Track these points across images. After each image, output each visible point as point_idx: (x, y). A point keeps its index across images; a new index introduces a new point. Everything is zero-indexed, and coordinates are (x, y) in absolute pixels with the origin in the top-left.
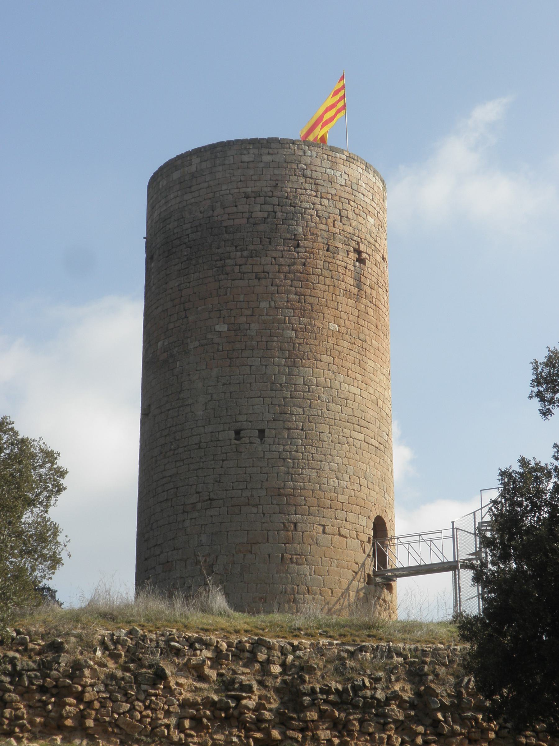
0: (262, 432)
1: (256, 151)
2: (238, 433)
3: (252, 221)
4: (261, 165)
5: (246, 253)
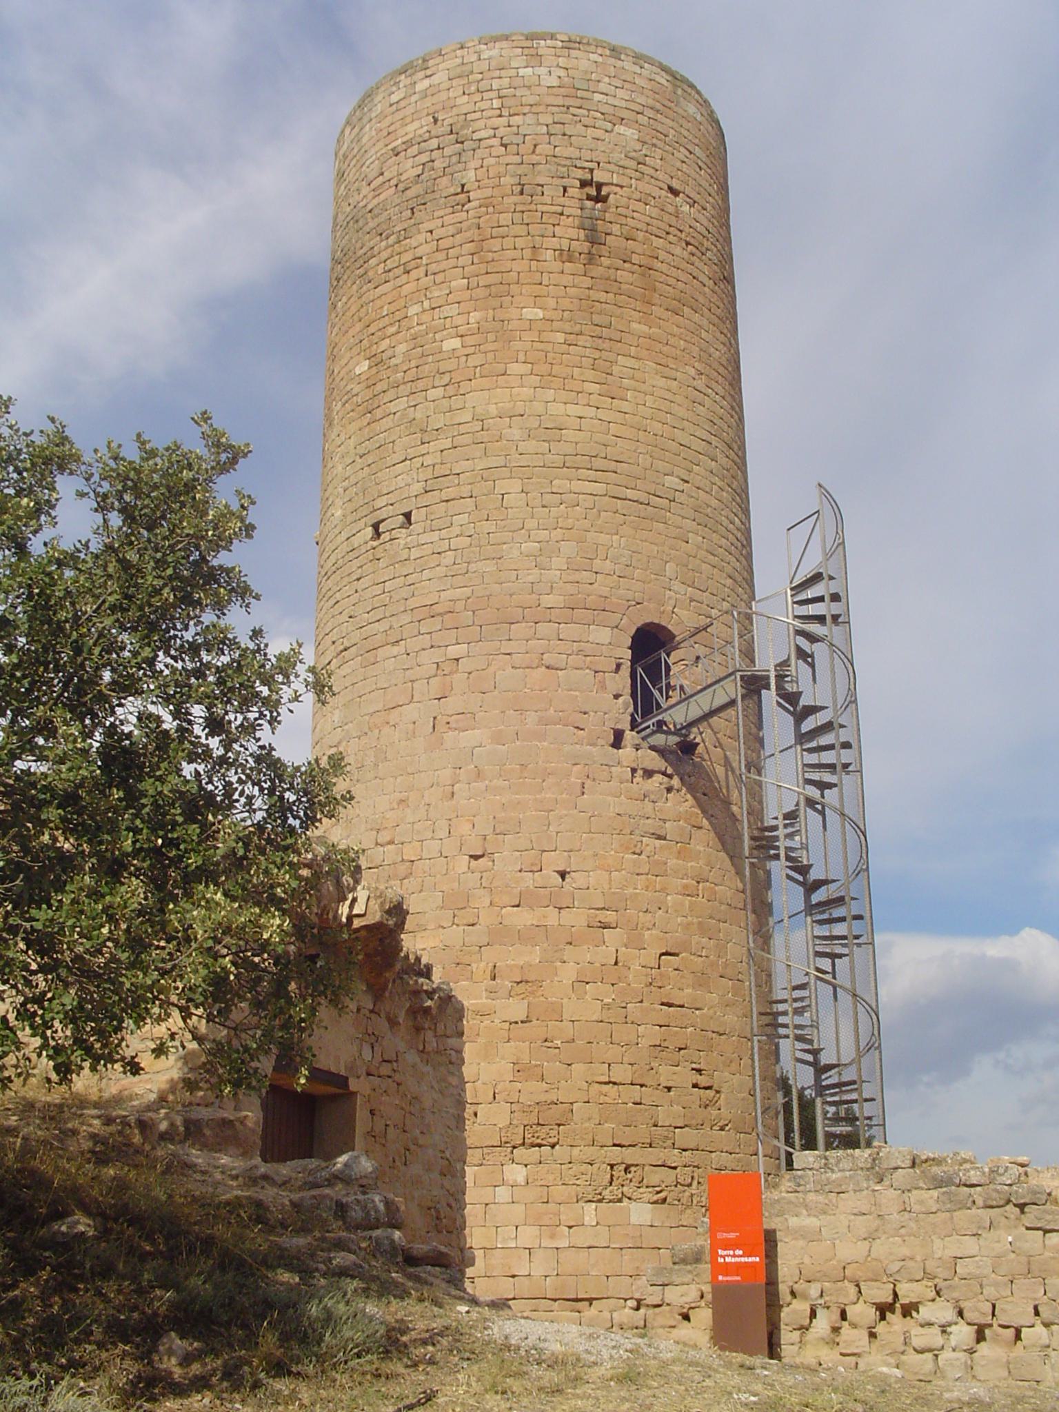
0: (408, 516)
1: (408, 81)
2: (376, 527)
3: (401, 187)
4: (413, 99)
5: (392, 239)
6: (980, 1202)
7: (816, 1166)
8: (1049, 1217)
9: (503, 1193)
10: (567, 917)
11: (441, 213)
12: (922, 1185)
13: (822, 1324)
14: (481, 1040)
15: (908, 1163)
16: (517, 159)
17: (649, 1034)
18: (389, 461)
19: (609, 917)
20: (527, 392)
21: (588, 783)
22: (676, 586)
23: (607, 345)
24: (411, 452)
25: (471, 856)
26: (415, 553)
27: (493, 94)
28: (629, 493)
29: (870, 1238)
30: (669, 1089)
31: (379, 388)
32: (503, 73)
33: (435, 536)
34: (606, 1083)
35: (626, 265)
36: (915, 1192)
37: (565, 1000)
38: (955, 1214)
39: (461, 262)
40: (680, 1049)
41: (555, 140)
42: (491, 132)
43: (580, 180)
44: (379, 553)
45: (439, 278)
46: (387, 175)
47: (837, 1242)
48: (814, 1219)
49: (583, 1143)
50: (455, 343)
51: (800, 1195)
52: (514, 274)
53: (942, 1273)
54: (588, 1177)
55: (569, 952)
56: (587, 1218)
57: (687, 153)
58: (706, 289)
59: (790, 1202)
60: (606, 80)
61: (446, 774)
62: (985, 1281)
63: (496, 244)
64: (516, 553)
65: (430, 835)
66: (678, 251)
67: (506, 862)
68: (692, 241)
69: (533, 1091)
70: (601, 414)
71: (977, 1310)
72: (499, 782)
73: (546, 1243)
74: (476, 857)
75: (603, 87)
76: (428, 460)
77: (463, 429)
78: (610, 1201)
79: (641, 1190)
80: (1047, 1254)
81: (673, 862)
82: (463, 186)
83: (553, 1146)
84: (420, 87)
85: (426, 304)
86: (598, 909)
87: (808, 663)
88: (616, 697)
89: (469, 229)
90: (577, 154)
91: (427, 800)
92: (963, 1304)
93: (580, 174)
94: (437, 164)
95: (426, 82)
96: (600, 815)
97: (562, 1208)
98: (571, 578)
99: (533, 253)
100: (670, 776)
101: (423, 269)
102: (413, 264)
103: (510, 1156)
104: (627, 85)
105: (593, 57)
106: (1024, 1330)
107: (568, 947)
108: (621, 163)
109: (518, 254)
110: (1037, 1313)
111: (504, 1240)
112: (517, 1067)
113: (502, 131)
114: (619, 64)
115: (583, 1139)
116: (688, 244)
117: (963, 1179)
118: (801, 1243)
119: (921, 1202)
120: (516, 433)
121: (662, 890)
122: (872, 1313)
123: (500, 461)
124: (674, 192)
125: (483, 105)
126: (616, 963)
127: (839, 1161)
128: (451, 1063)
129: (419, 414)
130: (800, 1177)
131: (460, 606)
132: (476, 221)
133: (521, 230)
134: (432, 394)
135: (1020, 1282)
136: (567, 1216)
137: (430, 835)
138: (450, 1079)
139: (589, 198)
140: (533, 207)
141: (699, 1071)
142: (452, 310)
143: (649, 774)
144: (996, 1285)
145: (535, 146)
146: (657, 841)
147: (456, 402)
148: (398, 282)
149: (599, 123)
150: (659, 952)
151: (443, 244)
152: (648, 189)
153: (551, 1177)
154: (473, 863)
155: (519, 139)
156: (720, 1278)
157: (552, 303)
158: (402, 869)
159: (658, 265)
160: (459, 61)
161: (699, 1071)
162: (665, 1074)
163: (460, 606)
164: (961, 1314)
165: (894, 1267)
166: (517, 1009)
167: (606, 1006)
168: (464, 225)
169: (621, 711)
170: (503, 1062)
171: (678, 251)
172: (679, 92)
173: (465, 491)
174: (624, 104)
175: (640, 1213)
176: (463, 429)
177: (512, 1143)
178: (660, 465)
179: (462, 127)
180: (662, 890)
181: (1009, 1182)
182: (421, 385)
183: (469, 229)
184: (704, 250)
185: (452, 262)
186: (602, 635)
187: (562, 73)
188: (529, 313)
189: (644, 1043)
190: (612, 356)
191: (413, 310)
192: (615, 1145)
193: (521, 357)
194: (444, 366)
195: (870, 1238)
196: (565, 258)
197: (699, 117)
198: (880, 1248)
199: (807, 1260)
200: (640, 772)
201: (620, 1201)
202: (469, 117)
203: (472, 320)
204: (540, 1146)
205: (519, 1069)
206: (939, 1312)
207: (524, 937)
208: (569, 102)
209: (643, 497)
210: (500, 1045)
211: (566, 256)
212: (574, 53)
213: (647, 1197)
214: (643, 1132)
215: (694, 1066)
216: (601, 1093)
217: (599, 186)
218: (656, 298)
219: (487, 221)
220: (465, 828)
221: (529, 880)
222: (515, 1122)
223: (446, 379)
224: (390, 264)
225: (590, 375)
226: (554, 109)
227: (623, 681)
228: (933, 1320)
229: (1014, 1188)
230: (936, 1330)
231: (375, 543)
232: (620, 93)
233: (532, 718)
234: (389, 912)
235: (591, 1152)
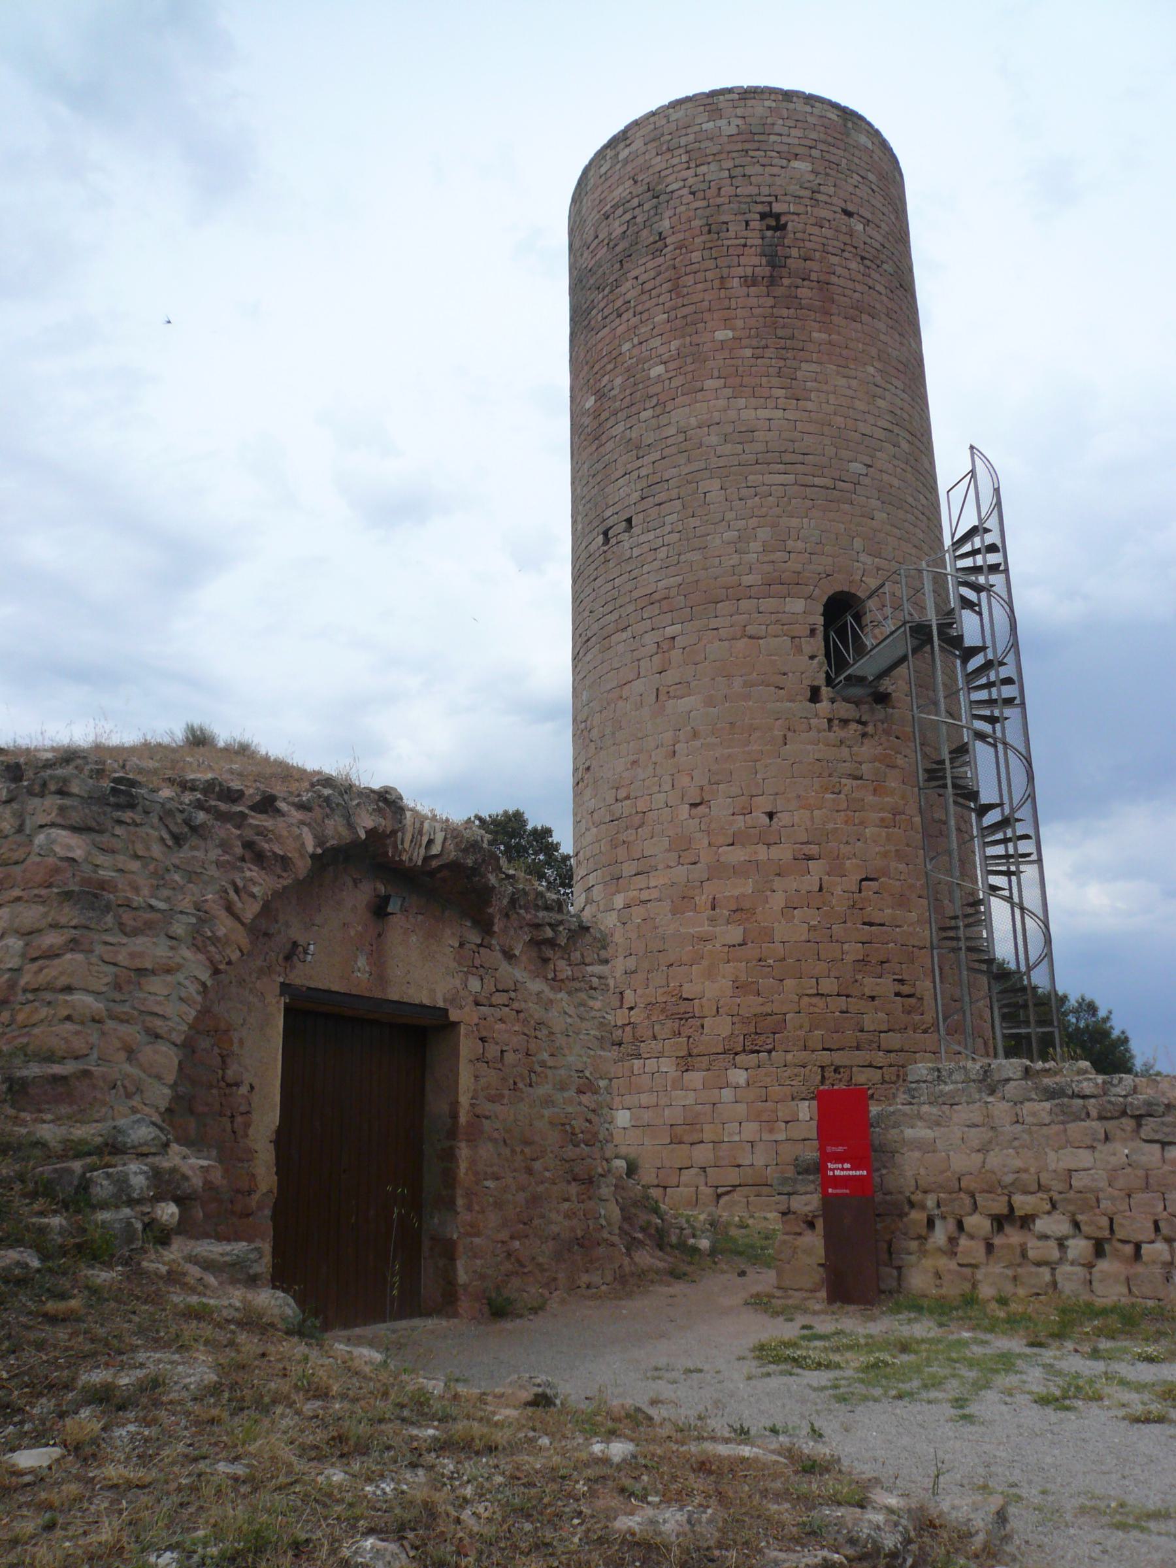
0: (629, 521)
2: (606, 534)
3: (611, 244)
4: (618, 167)
5: (607, 290)
6: (1094, 1113)
7: (929, 1078)
8: (1166, 1130)
9: (727, 1094)
10: (776, 852)
11: (644, 260)
12: (1034, 1097)
13: (940, 1236)
14: (705, 963)
15: (1019, 1074)
16: (704, 203)
17: (853, 951)
18: (613, 478)
19: (814, 849)
20: (722, 403)
21: (789, 734)
22: (863, 557)
23: (790, 354)
24: (630, 467)
25: (691, 805)
26: (636, 552)
27: (682, 151)
28: (817, 481)
29: (984, 1149)
30: (873, 998)
31: (603, 417)
32: (689, 130)
33: (651, 535)
34: (814, 995)
35: (806, 283)
36: (1027, 1104)
37: (776, 924)
38: (1068, 1126)
39: (661, 300)
41: (736, 182)
42: (681, 184)
43: (760, 213)
44: (609, 555)
45: (645, 316)
46: (601, 237)
47: (951, 1153)
48: (929, 1131)
50: (660, 369)
51: (915, 1107)
52: (706, 303)
53: (1057, 1186)
55: (778, 883)
56: (801, 1115)
57: (860, 179)
58: (884, 298)
59: (905, 1114)
60: (780, 122)
61: (669, 735)
62: (1101, 1195)
63: (689, 280)
64: (718, 542)
65: (656, 789)
66: (853, 265)
67: (720, 808)
68: (867, 255)
69: (751, 1004)
70: (788, 415)
71: (1096, 1224)
72: (713, 740)
73: (766, 1137)
74: (694, 805)
75: (777, 129)
76: (643, 472)
77: (670, 441)
80: (1167, 1168)
81: (870, 798)
82: (660, 234)
83: (769, 1052)
84: (622, 156)
85: (636, 341)
86: (802, 844)
87: (975, 611)
88: (812, 658)
89: (667, 270)
90: (756, 191)
91: (654, 759)
92: (1079, 1218)
93: (760, 208)
94: (638, 220)
95: (627, 151)
96: (801, 762)
98: (766, 559)
99: (722, 283)
100: (864, 724)
101: (632, 311)
102: (624, 308)
104: (799, 124)
105: (767, 103)
106: (1144, 1246)
107: (777, 878)
108: (797, 193)
109: (709, 284)
110: (1157, 1228)
111: (730, 1135)
112: (736, 984)
113: (691, 181)
114: (792, 106)
115: (794, 1045)
116: (863, 258)
117: (1076, 1090)
118: (917, 1154)
119: (1034, 1114)
120: (714, 439)
121: (861, 823)
122: (987, 1224)
123: (702, 465)
124: (849, 214)
125: (675, 161)
126: (821, 890)
127: (951, 1073)
128: (591, 988)
129: (634, 434)
130: (914, 1089)
131: (673, 592)
132: (671, 262)
133: (710, 264)
134: (645, 415)
135: (1138, 1197)
136: (783, 1111)
137: (656, 789)
138: (591, 1003)
139: (769, 228)
140: (720, 243)
141: (901, 981)
142: (657, 342)
143: (845, 722)
144: (1113, 1199)
145: (719, 189)
146: (855, 782)
147: (664, 420)
148: (613, 325)
149: (775, 161)
150: (859, 878)
151: (648, 286)
152: (824, 213)
153: (769, 1080)
154: (694, 811)
155: (704, 186)
156: (830, 1190)
157: (739, 323)
158: (637, 820)
159: (834, 279)
160: (652, 127)
161: (901, 981)
162: (869, 984)
163: (673, 592)
164: (1076, 1225)
165: (1008, 1179)
166: (734, 934)
167: (812, 928)
168: (663, 268)
169: (816, 671)
171: (853, 265)
172: (850, 125)
173: (674, 493)
174: (796, 141)
176: (670, 441)
178: (845, 454)
179: (658, 183)
180: (861, 823)
181: (1124, 1093)
182: (634, 410)
183: (667, 270)
184: (878, 262)
185: (654, 301)
186: (797, 605)
187: (740, 122)
188: (721, 335)
189: (849, 958)
190: (795, 364)
191: (626, 347)
192: (824, 1049)
193: (716, 374)
194: (652, 390)
195: (984, 1149)
196: (749, 283)
197: (870, 146)
198: (994, 1160)
199: (922, 1171)
200: (836, 722)
202: (663, 174)
203: (673, 348)
204: (758, 1052)
205: (740, 987)
206: (1053, 1225)
207: (738, 871)
208: (747, 146)
209: (829, 482)
211: (750, 281)
212: (750, 103)
216: (811, 1005)
217: (777, 216)
218: (834, 310)
219: (681, 261)
220: (685, 780)
221: (740, 822)
222: (737, 1032)
223: (654, 401)
224: (606, 312)
225: (775, 381)
226: (734, 155)
227: (818, 644)
228: (1049, 1233)
229: (1130, 1099)
230: (1052, 1243)
231: (605, 548)
232: (793, 132)
233: (738, 682)
234: (465, 851)
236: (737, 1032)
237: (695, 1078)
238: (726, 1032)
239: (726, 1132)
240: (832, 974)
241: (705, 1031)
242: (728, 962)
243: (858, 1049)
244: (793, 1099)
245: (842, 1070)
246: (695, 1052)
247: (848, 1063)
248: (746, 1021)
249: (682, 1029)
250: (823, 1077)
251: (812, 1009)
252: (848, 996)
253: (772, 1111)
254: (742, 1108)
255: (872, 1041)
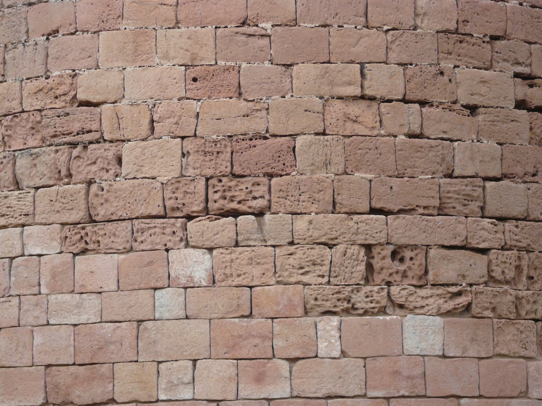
9: (168, 301)
30: (473, 109)
40: (495, 38)
49: (314, 208)
54: (326, 268)
69: (223, 115)
78: (366, 313)
79: (423, 292)
83: (260, 214)
97: (277, 326)
103: (180, 234)
111: (172, 386)
153: (256, 271)
162: (468, 83)
170: (167, 64)
175: (422, 333)
177: (186, 211)
192: (373, 211)
201: (383, 311)
204: (236, 214)
210: (161, 32)
213: (434, 303)
214: (425, 187)
215: (520, 69)
216: (348, 118)
222: (190, 172)
235: (328, 224)
236: (190, 172)
237: (100, 268)
238: (167, 171)
239: (162, 385)
240: (393, 57)
241: (124, 171)
242: (177, 24)
243: (441, 211)
244: (306, 313)
245: (408, 254)
246: (101, 213)
247: (421, 239)
248: (210, 151)
249: (75, 164)
250: (370, 267)
251: (350, 128)
252: (423, 103)
253: (263, 337)
254: (198, 330)
255: (470, 198)
